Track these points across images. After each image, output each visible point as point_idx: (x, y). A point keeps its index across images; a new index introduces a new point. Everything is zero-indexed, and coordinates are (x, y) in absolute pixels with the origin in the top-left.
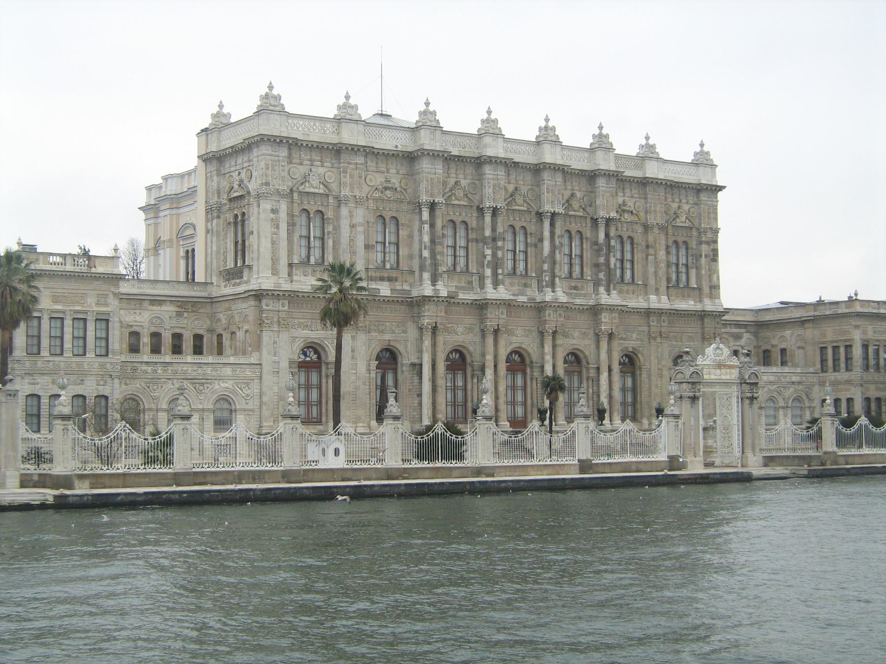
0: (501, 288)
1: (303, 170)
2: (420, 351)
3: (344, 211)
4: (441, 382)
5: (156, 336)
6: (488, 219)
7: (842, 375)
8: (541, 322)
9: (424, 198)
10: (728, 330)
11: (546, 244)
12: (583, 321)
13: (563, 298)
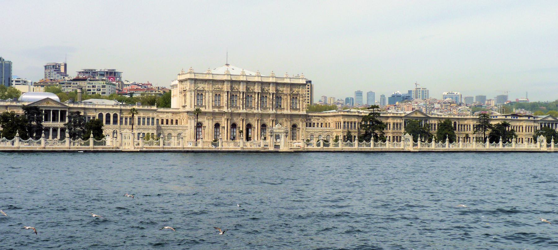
3: (207, 94)
4: (229, 131)
6: (242, 94)
7: (339, 130)
11: (256, 99)
13: (260, 112)
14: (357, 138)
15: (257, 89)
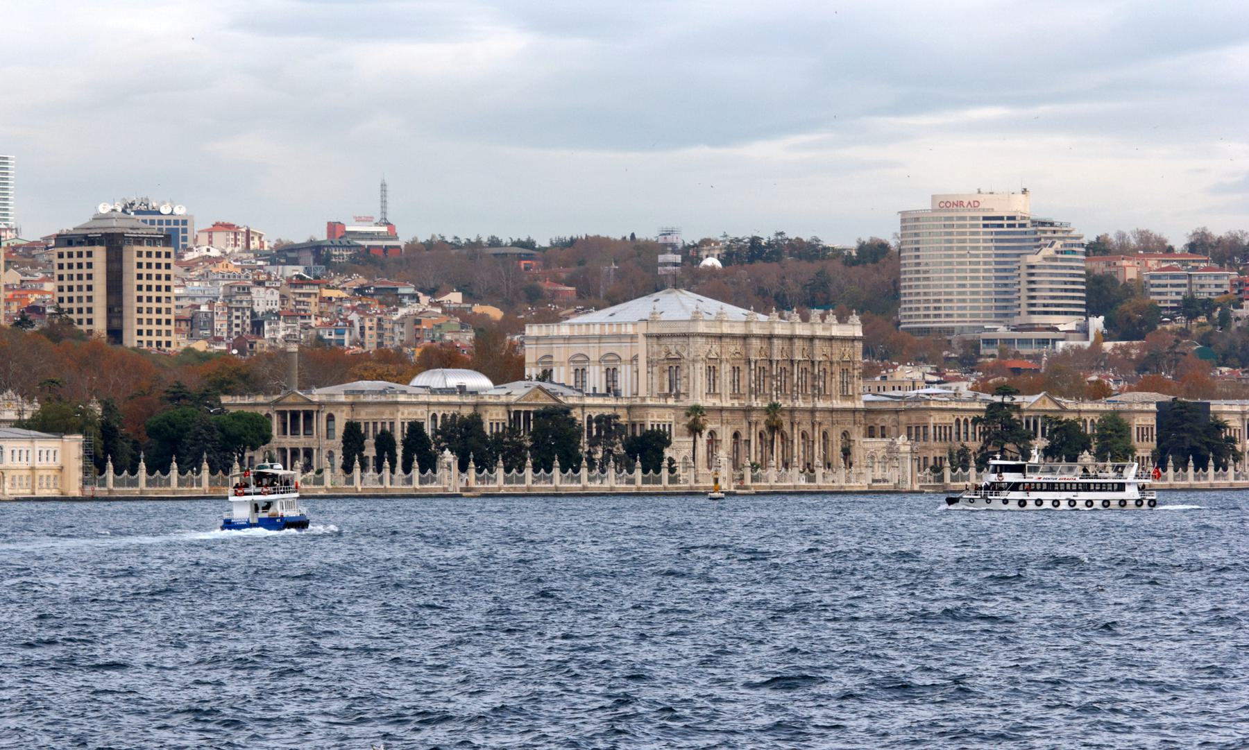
2: (750, 434)
8: (792, 417)
9: (753, 358)
12: (807, 416)
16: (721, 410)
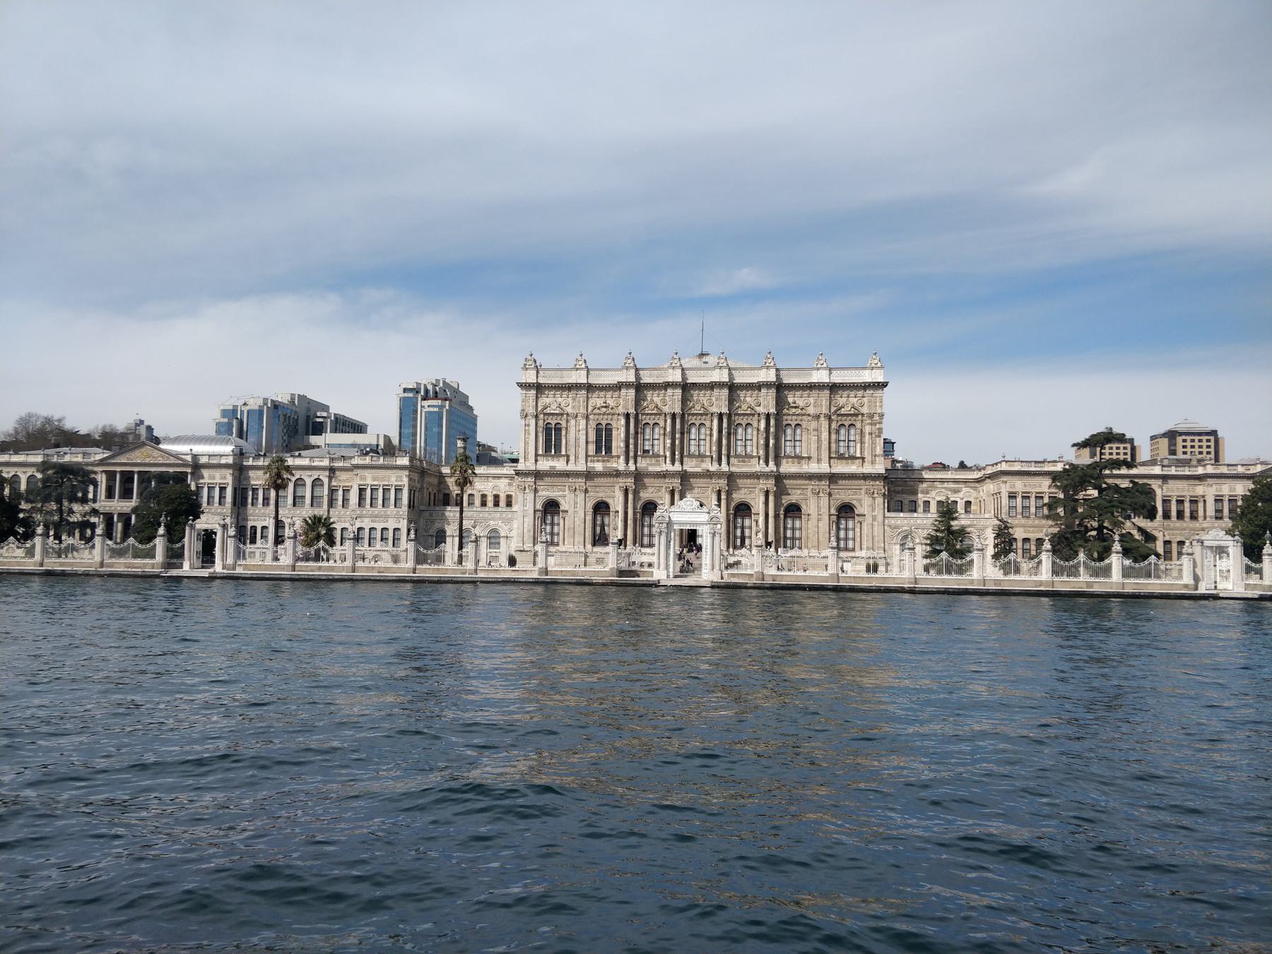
0: (677, 464)
1: (548, 401)
3: (573, 422)
5: (496, 497)
6: (669, 421)
10: (945, 485)
14: (1047, 545)
15: (718, 402)
16: (567, 474)
